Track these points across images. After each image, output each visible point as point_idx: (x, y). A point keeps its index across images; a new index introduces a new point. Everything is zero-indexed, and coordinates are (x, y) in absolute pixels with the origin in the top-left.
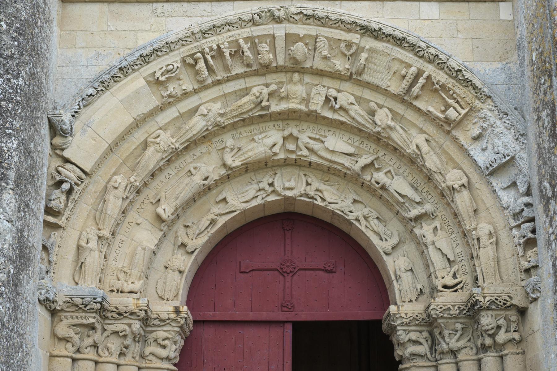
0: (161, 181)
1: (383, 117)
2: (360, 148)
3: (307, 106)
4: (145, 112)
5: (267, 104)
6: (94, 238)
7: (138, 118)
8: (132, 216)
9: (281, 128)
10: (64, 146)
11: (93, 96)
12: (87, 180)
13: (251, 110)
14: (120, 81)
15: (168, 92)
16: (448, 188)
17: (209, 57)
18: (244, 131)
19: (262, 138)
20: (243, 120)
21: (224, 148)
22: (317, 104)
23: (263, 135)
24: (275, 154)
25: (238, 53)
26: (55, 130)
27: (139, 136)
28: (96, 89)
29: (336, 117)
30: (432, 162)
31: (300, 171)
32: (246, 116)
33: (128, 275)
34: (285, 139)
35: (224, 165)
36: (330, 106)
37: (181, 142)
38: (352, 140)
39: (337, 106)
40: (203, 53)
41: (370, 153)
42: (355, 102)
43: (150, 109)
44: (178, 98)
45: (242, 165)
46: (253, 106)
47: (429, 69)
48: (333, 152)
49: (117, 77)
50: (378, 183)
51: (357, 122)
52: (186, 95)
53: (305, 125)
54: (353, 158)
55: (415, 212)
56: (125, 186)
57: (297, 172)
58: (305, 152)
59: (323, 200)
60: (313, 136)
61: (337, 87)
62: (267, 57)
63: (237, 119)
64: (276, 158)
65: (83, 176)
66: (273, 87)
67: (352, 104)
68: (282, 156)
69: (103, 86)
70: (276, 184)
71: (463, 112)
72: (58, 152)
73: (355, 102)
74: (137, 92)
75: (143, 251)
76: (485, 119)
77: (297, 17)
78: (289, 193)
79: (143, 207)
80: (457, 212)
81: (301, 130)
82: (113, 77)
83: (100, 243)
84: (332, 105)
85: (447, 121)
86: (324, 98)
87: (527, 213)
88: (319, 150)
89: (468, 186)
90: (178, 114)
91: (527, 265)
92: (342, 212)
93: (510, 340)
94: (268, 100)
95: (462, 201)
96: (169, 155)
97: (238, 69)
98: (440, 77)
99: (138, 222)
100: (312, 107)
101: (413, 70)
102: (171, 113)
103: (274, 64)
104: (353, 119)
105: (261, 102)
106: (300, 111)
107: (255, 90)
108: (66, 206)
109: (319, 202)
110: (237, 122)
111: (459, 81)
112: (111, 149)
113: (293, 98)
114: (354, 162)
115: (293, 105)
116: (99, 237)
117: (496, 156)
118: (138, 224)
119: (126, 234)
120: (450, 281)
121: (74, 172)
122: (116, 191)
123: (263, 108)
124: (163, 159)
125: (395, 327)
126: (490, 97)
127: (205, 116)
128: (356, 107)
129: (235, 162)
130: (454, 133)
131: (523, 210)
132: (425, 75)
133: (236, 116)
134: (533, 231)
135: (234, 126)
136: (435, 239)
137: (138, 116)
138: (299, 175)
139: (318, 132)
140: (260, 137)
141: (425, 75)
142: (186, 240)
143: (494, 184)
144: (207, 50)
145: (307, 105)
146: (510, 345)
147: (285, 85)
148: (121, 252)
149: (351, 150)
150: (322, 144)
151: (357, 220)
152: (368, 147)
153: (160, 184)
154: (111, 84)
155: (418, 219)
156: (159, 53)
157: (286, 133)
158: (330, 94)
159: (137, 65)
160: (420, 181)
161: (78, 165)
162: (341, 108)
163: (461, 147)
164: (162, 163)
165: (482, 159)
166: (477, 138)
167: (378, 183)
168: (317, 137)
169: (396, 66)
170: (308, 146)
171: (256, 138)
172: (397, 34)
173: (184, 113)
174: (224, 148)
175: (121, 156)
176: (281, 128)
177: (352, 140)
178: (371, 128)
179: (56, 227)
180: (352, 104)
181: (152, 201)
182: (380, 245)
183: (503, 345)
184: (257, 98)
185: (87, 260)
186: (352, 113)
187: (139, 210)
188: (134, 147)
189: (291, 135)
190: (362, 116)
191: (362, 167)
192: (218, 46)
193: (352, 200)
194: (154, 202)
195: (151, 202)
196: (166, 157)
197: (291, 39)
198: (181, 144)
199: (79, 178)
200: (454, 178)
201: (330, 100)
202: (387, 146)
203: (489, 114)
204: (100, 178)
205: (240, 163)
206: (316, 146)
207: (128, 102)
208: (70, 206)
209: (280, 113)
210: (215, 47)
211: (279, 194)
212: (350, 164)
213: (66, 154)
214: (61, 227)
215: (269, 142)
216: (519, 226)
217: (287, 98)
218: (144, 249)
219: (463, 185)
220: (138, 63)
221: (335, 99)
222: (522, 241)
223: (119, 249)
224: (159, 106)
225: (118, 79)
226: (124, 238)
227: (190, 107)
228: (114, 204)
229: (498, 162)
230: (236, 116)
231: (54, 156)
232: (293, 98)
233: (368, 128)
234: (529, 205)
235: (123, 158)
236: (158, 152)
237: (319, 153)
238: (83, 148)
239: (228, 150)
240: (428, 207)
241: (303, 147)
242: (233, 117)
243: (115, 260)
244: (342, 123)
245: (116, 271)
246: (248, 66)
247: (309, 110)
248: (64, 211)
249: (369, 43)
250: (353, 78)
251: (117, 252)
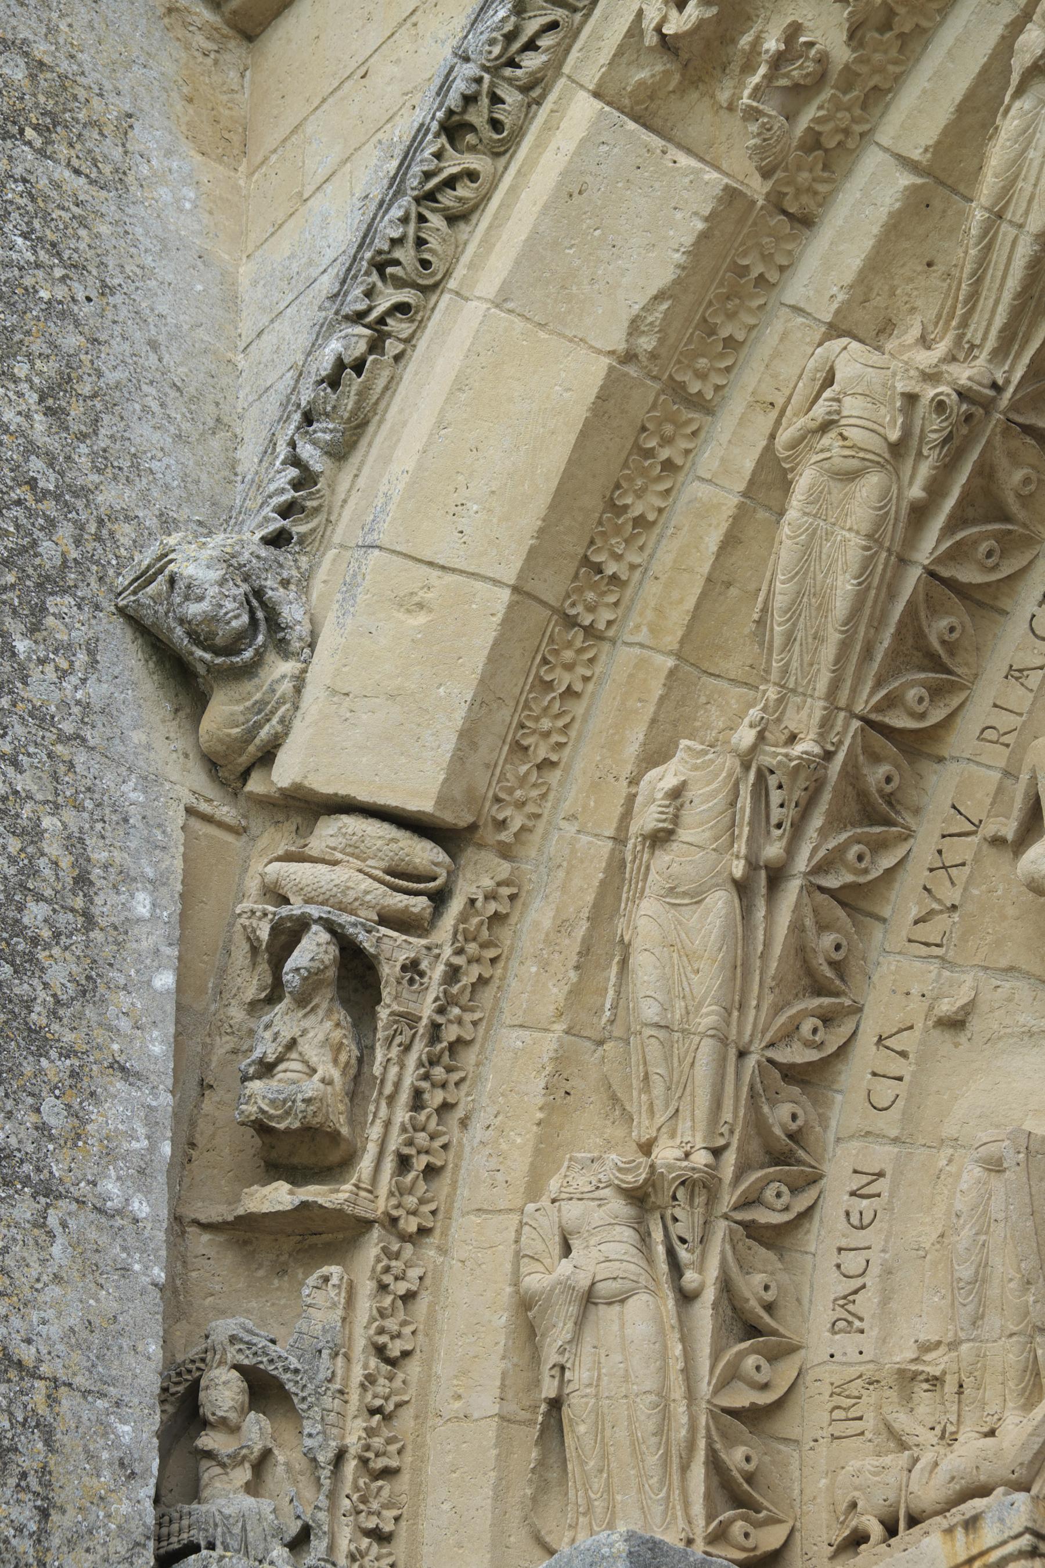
0: (1016, 673)
4: (664, 276)
6: (599, 1216)
7: (646, 343)
8: (898, 982)
10: (264, 733)
11: (358, 367)
12: (477, 877)
14: (486, 198)
26: (187, 665)
27: (725, 454)
28: (359, 317)
33: (950, 1387)
37: (991, 343)
43: (688, 240)
44: (849, 77)
49: (451, 183)
56: (720, 799)
65: (424, 854)
69: (400, 283)
72: (255, 785)
74: (571, 191)
75: (996, 1183)
79: (951, 895)
82: (431, 196)
83: (658, 1235)
90: (906, 180)
96: (948, 468)
99: (946, 1007)
102: (870, 194)
108: (359, 1082)
112: (571, 622)
116: (641, 1199)
118: (954, 1024)
119: (888, 1124)
121: (356, 851)
122: (663, 859)
124: (919, 513)
137: (635, 327)
148: (874, 1255)
153: (1018, 697)
154: (433, 243)
159: (531, 46)
161: (363, 795)
164: (929, 545)
173: (938, 148)
175: (653, 630)
179: (318, 1238)
181: (990, 829)
185: (580, 1376)
187: (931, 931)
188: (712, 541)
194: (1009, 830)
195: (997, 841)
196: (936, 489)
198: (1000, 353)
199: (401, 875)
204: (570, 829)
207: (541, 292)
208: (398, 1068)
213: (286, 771)
214: (367, 1224)
218: (995, 1166)
220: (532, 27)
223: (860, 1238)
224: (731, 195)
225: (464, 190)
226: (881, 1156)
227: (960, 85)
228: (682, 945)
231: (255, 825)
235: (671, 640)
236: (850, 476)
238: (376, 700)
243: (847, 1322)
245: (870, 1397)
248: (357, 1121)
251: (853, 1262)
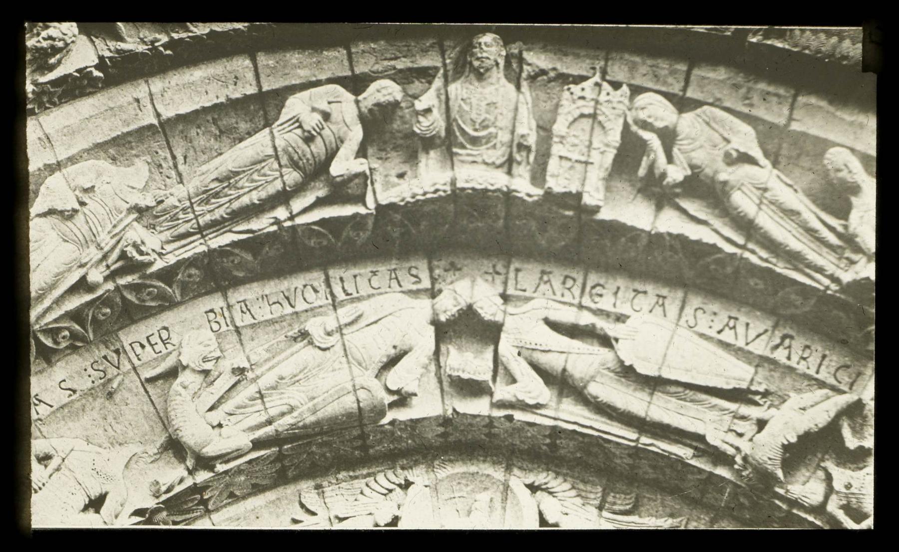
2: (773, 362)
3: (539, 175)
5: (360, 166)
9: (426, 283)
13: (283, 197)
18: (257, 299)
19: (340, 329)
20: (255, 243)
21: (172, 374)
23: (346, 313)
24: (402, 399)
29: (669, 223)
31: (508, 469)
32: (262, 224)
34: (444, 331)
35: (175, 447)
36: (642, 172)
38: (741, 329)
39: (676, 174)
41: (822, 384)
42: (756, 152)
45: (257, 444)
46: (292, 177)
48: (654, 384)
53: (527, 277)
54: (745, 410)
57: (498, 473)
60: (568, 316)
61: (676, 88)
63: (227, 239)
64: (403, 415)
67: (746, 159)
68: (428, 405)
73: (756, 152)
81: (511, 291)
84: (651, 167)
86: (615, 137)
88: (593, 378)
94: (362, 152)
100: (560, 180)
105: (331, 155)
106: (508, 196)
110: (222, 252)
113: (475, 141)
114: (748, 428)
115: (476, 173)
123: (341, 191)
127: (68, 216)
128: (765, 173)
133: (217, 225)
135: (214, 275)
138: (507, 487)
139: (587, 301)
140: (332, 325)
145: (539, 175)
147: (438, 82)
149: (738, 374)
150: (605, 354)
152: (814, 360)
157: (448, 305)
158: (642, 115)
168: (585, 319)
170: (543, 359)
171: (314, 326)
174: (172, 374)
176: (426, 283)
177: (741, 329)
178: (830, 269)
180: (746, 159)
184: (309, 139)
186: (743, 202)
190: (791, 214)
191: (787, 448)
201: (643, 147)
205: (245, 441)
206: (582, 360)
209: (411, 212)
212: (732, 438)
215: (373, 344)
217: (448, 143)
230: (217, 225)
232: (475, 141)
233: (820, 270)
237: (593, 389)
239: (185, 377)
241: (520, 368)
242: (201, 231)
244: (697, 251)
247: (549, 194)
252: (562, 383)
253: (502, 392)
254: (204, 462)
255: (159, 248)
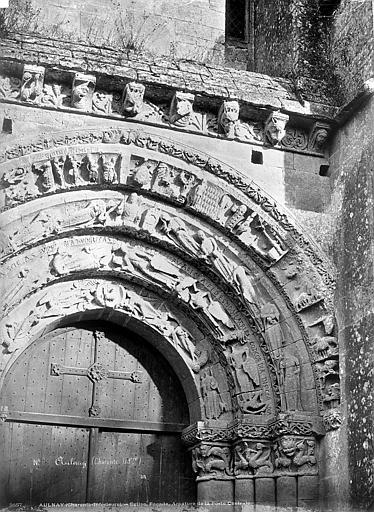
1: (208, 246)
3: (140, 225)
15: (15, 195)
16: (262, 319)
17: (57, 166)
22: (150, 226)
24: (102, 266)
25: (85, 167)
29: (165, 238)
30: (249, 292)
39: (169, 230)
40: (52, 162)
47: (257, 209)
50: (195, 305)
51: (184, 246)
52: (30, 198)
55: (225, 337)
58: (130, 268)
59: (140, 314)
62: (110, 175)
63: (73, 229)
64: (102, 269)
66: (113, 204)
68: (108, 268)
70: (97, 293)
71: (284, 253)
76: (300, 262)
77: (144, 142)
78: (110, 304)
80: (267, 342)
85: (268, 259)
87: (331, 351)
89: (280, 320)
91: (328, 398)
92: (157, 327)
93: (307, 463)
95: (272, 331)
97: (80, 182)
98: (265, 218)
100: (145, 227)
101: (244, 209)
103: (116, 182)
104: (181, 243)
107: (94, 203)
109: (137, 316)
111: (282, 224)
117: (309, 298)
120: (254, 404)
125: (200, 441)
126: (308, 244)
129: (63, 268)
130: (272, 270)
131: (327, 349)
132: (254, 215)
134: (336, 368)
135: (68, 235)
136: (243, 363)
141: (254, 215)
142: (9, 340)
143: (304, 321)
144: (57, 160)
145: (140, 225)
146: (306, 466)
151: (171, 337)
155: (229, 343)
156: (11, 156)
160: (232, 309)
162: (172, 232)
163: (276, 284)
165: (297, 298)
166: (293, 278)
167: (195, 305)
168: (144, 255)
169: (227, 201)
172: (232, 173)
182: (192, 364)
183: (300, 466)
189: (120, 250)
192: (67, 157)
193: (167, 318)
197: (139, 161)
200: (267, 310)
202: (206, 273)
203: (306, 257)
206: (143, 264)
210: (65, 159)
211: (99, 304)
216: (322, 362)
219: (276, 319)
221: (168, 222)
222: (324, 375)
229: (310, 302)
234: (333, 344)
240: (239, 333)
241: (129, 263)
246: (92, 181)
249: (208, 177)
250: (185, 207)
252: (138, 269)
253: (125, 268)
254: (59, 275)
255: (61, 230)
